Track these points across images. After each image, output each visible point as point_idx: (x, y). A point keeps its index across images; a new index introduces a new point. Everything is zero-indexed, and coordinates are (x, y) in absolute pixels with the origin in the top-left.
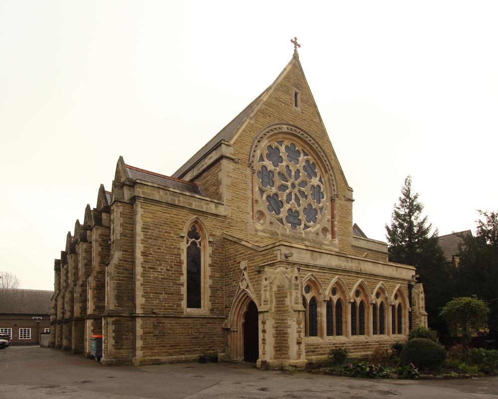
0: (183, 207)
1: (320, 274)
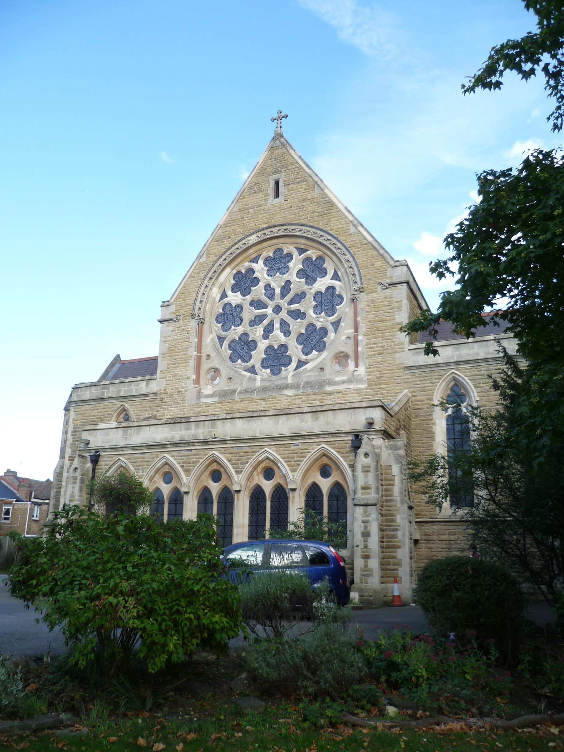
0: (109, 398)
1: (136, 456)
